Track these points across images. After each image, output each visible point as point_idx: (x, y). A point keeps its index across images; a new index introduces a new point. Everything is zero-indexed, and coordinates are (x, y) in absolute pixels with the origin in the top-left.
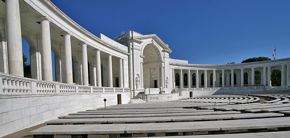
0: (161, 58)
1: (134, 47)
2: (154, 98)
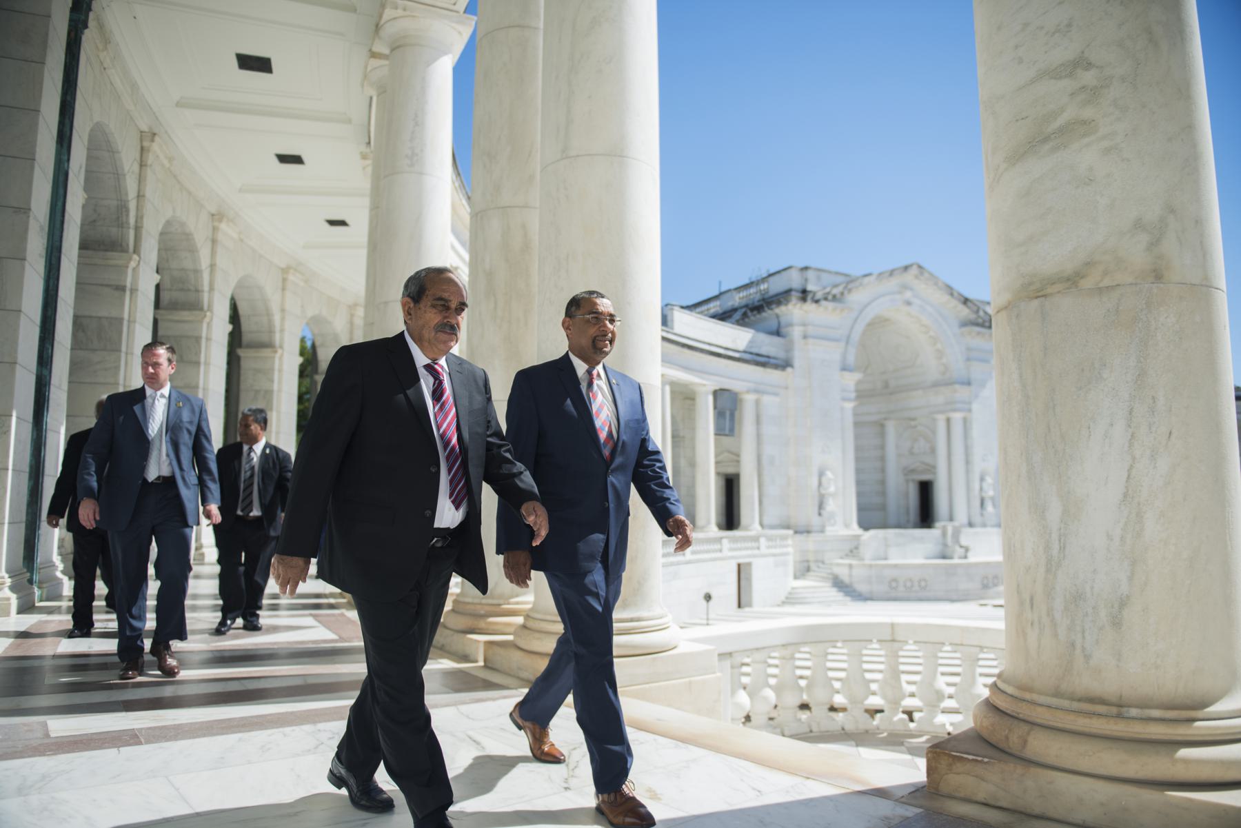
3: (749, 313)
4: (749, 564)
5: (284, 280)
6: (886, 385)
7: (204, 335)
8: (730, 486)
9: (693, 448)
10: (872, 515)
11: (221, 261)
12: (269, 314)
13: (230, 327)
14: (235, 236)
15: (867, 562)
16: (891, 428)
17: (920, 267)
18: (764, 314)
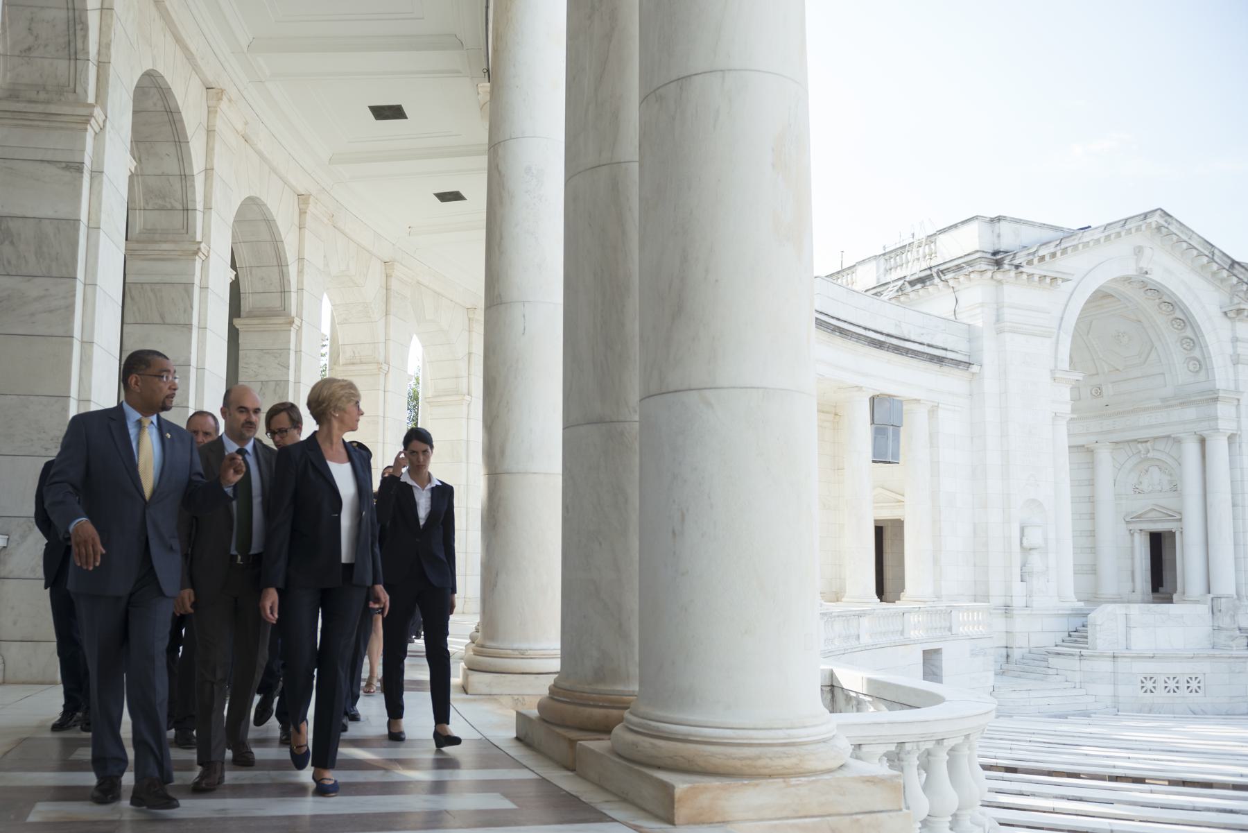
0: (1203, 373)
16: (1105, 456)
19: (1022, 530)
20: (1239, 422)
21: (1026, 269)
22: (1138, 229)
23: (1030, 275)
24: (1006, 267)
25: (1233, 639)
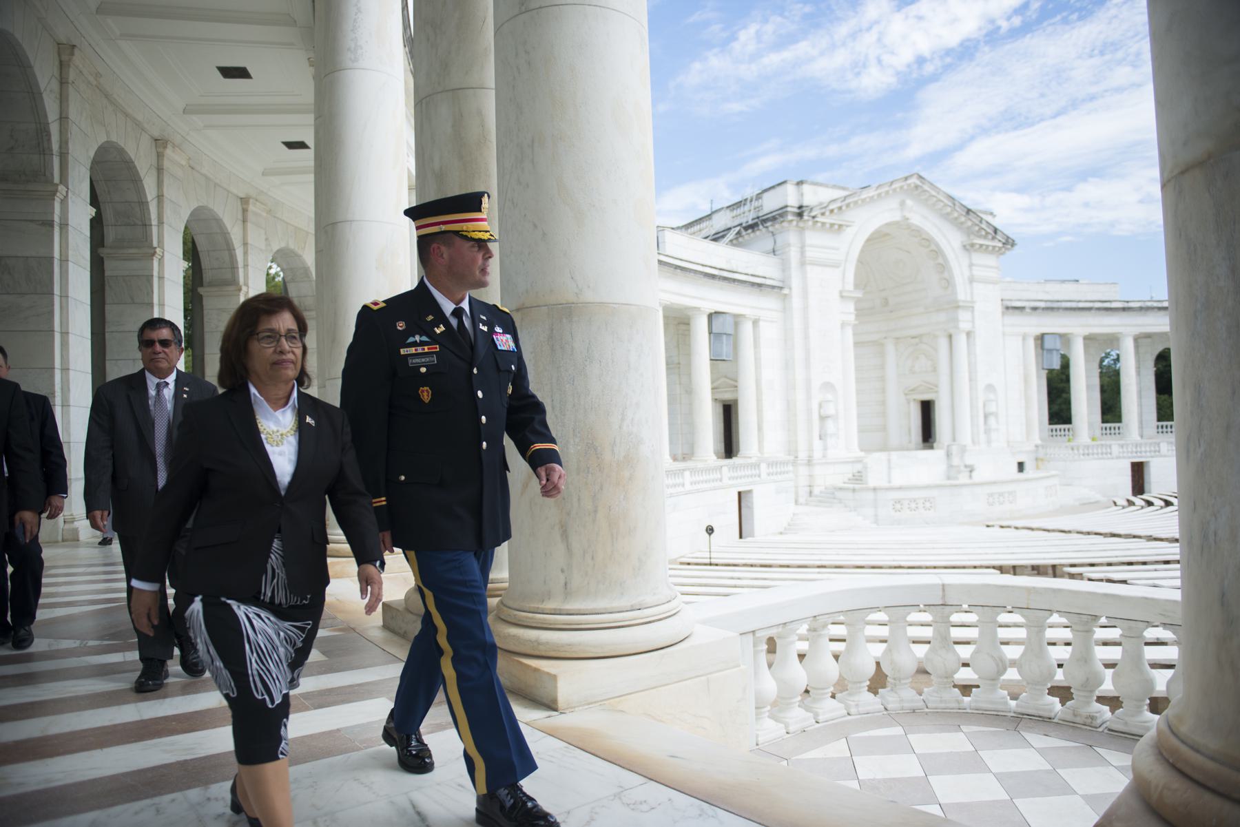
1: (811, 253)
2: (913, 505)
3: (744, 233)
4: (750, 492)
5: (245, 211)
6: (886, 302)
7: (155, 273)
8: (729, 413)
9: (689, 375)
10: (875, 438)
11: (170, 192)
12: (230, 249)
13: (185, 265)
14: (184, 163)
15: (871, 484)
16: (890, 348)
17: (920, 177)
18: (758, 233)
19: (820, 406)
20: (973, 322)
21: (820, 219)
22: (901, 188)
23: (823, 224)
24: (806, 218)
25: (959, 472)
